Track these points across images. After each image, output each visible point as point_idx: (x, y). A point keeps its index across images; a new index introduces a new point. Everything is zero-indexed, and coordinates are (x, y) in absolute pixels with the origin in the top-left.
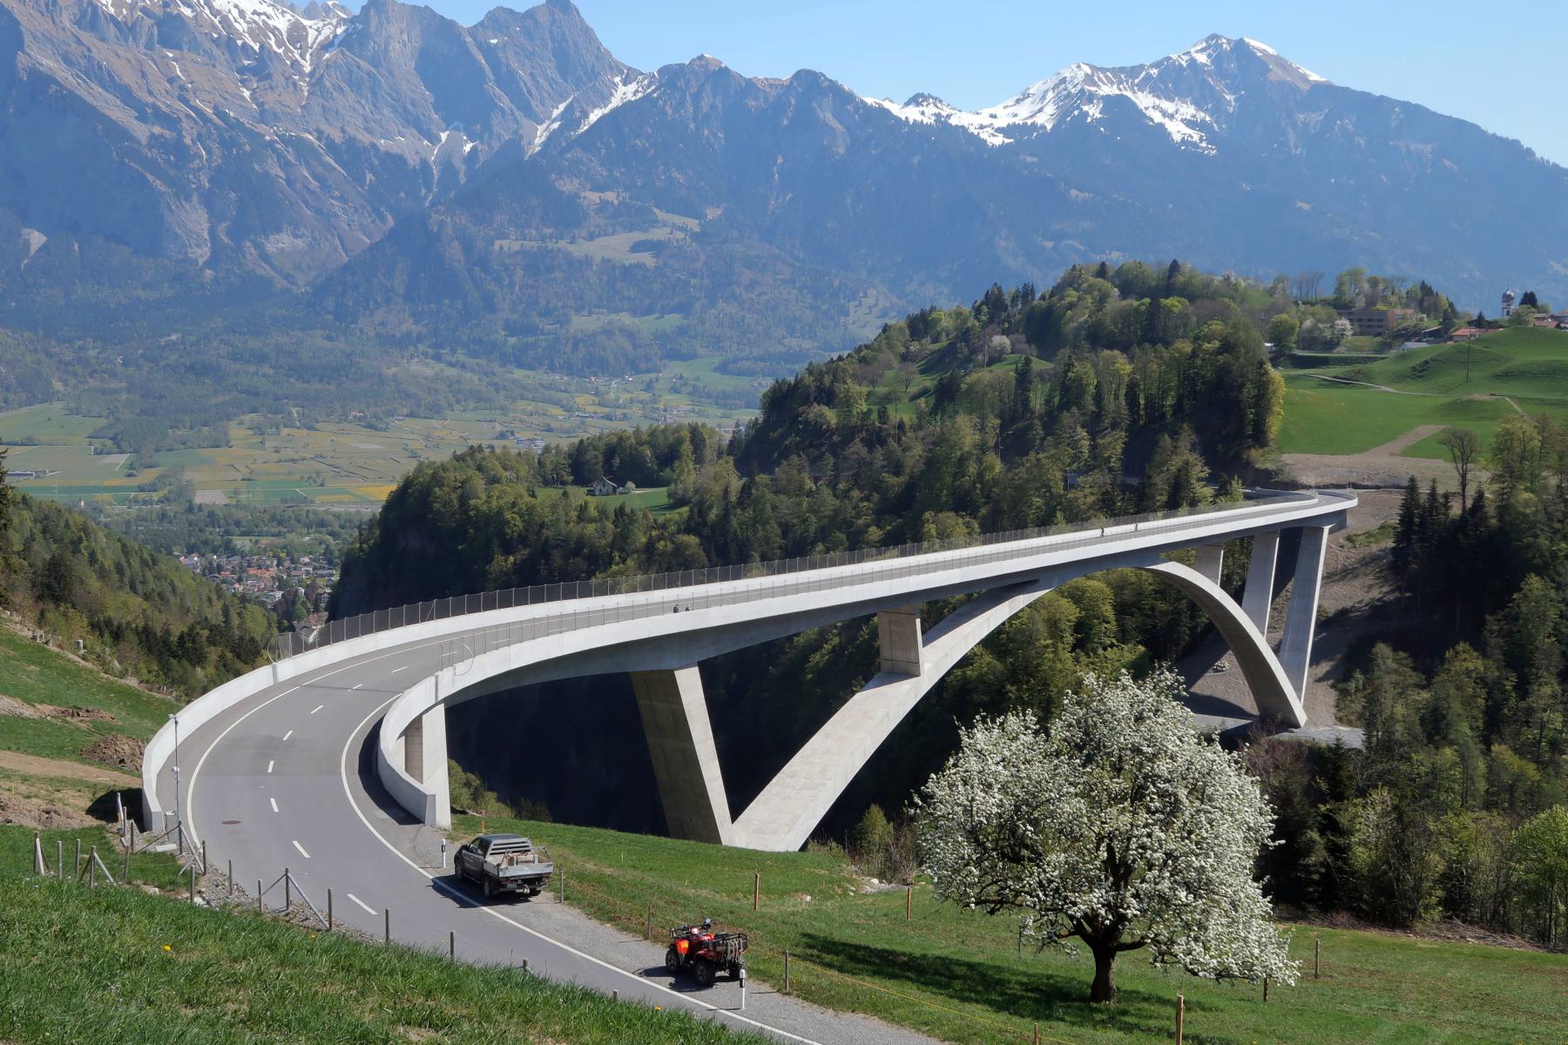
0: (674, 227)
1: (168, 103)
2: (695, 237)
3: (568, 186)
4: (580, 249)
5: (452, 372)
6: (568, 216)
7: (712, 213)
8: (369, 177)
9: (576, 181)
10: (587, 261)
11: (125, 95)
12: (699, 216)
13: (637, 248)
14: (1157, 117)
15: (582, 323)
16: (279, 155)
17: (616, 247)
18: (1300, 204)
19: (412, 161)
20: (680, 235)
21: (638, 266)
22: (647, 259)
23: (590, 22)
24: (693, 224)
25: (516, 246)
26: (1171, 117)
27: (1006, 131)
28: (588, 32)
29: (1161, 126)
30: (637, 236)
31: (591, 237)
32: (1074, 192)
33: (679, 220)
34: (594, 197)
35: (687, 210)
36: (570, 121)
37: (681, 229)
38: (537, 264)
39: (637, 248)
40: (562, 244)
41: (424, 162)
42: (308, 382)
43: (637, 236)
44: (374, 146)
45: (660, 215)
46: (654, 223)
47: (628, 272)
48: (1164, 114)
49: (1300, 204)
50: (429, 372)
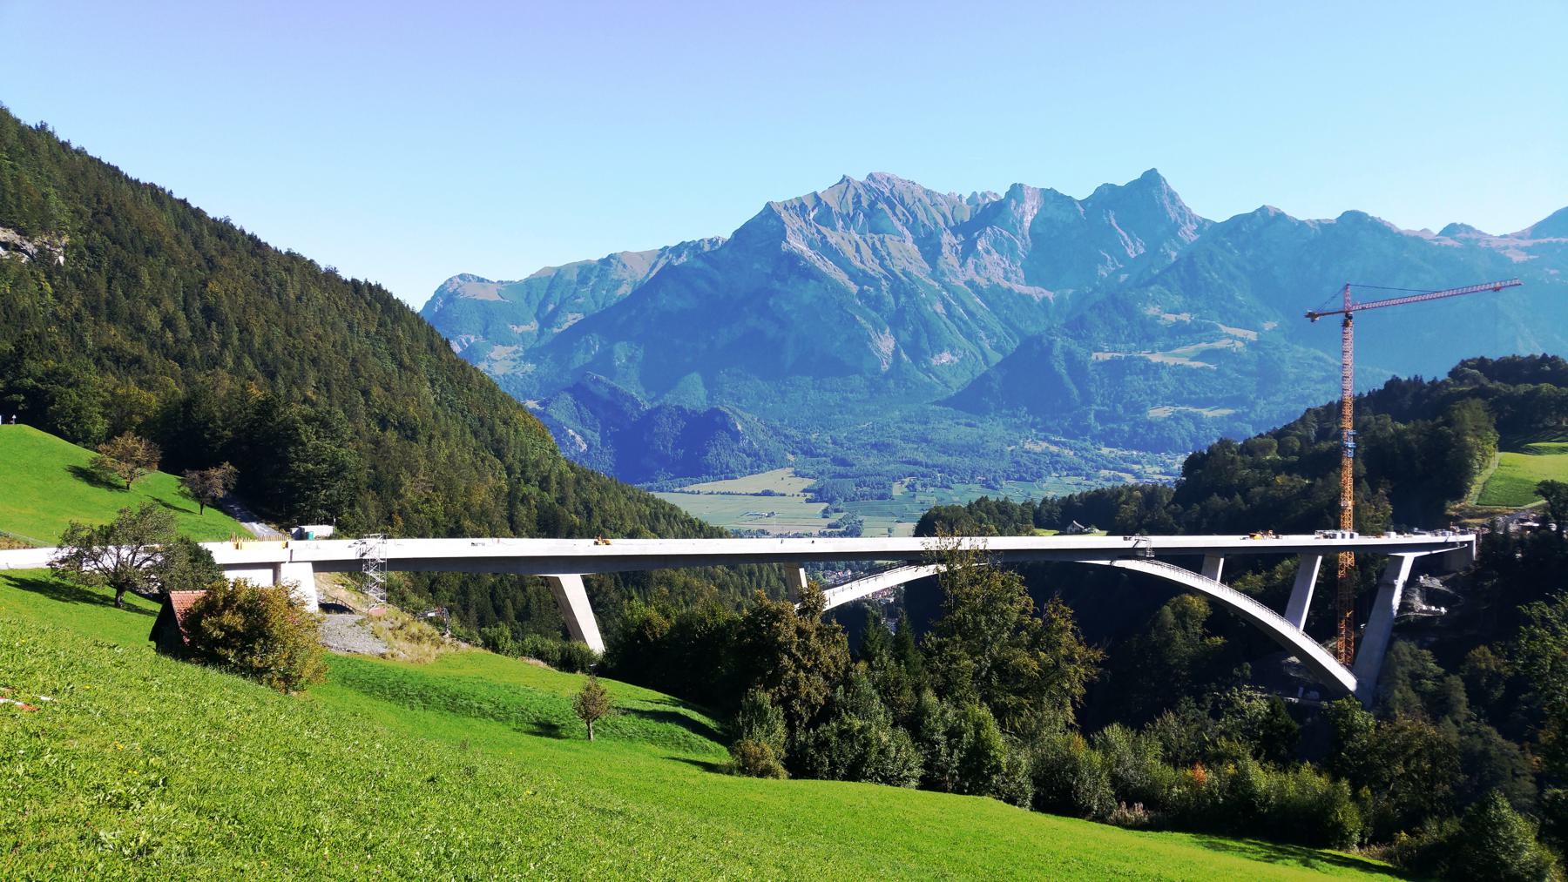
0: (1235, 338)
2: (1252, 346)
5: (1054, 449)
6: (1148, 334)
10: (1162, 365)
13: (1203, 356)
16: (943, 299)
23: (1175, 187)
24: (1252, 336)
25: (1108, 356)
28: (1173, 197)
33: (1240, 332)
34: (1172, 318)
37: (1242, 340)
38: (1116, 369)
42: (951, 455)
43: (1204, 346)
45: (1225, 329)
46: (1219, 337)
47: (1192, 373)
50: (1038, 449)
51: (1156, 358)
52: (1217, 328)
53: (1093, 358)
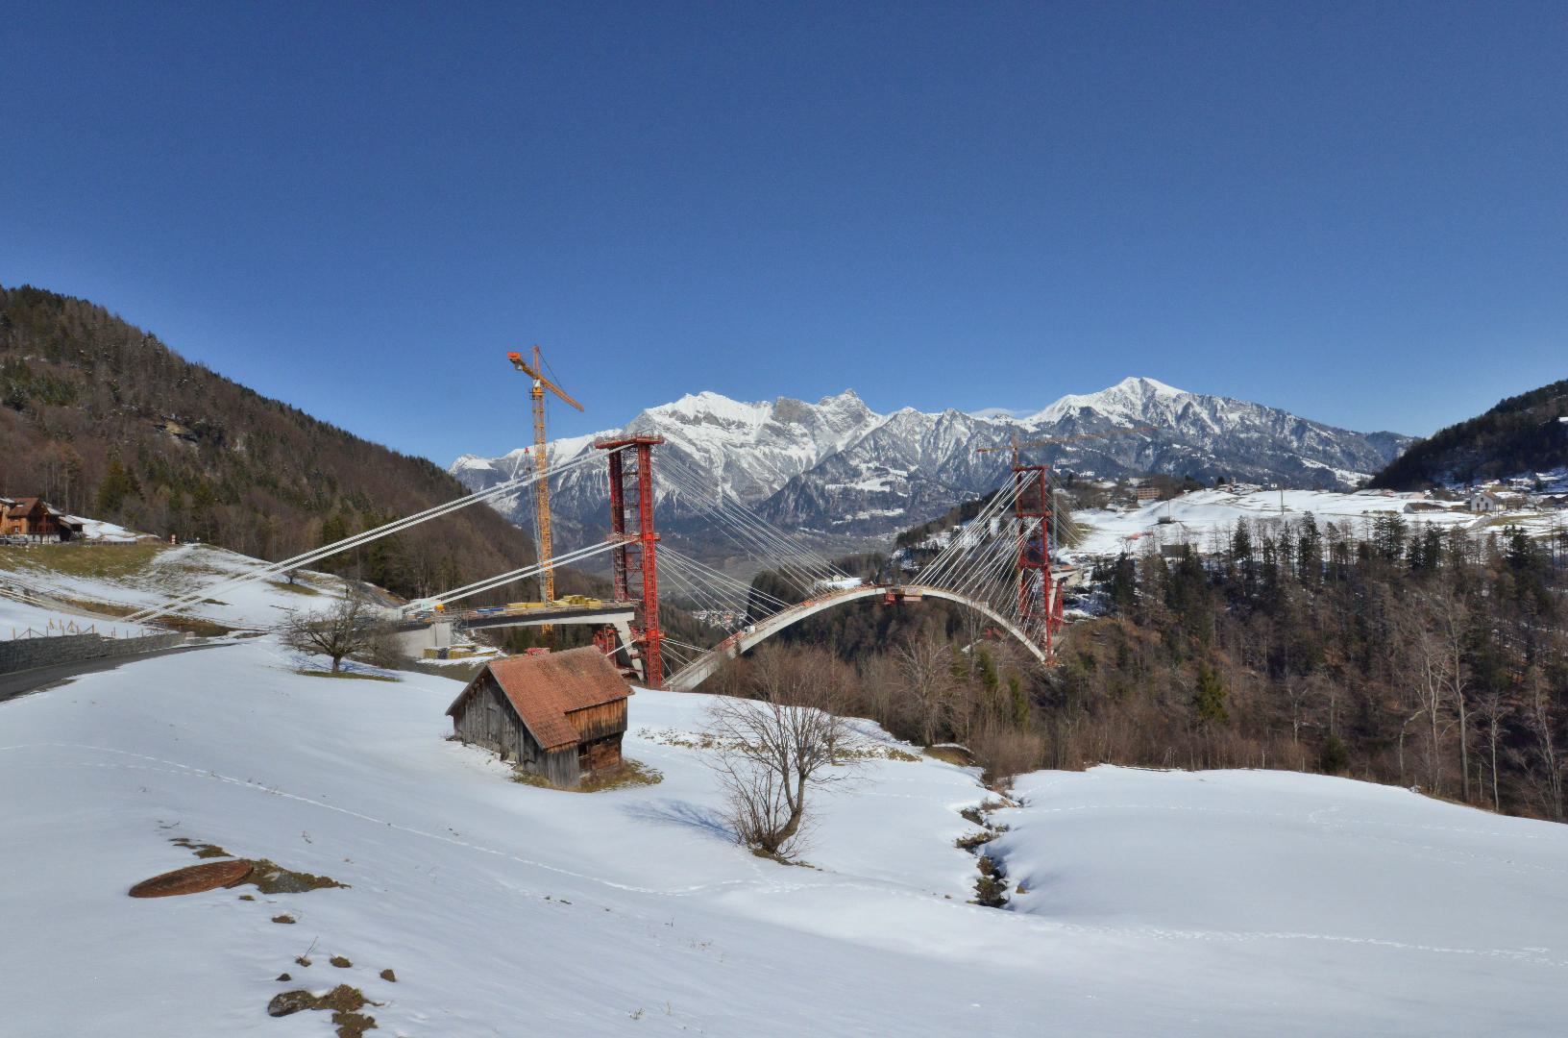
1: (705, 445)
3: (854, 463)
4: (861, 486)
6: (855, 474)
7: (913, 468)
8: (779, 464)
9: (857, 460)
10: (862, 491)
11: (690, 442)
12: (907, 470)
13: (882, 484)
14: (1105, 414)
15: (863, 515)
17: (873, 485)
18: (1175, 446)
19: (795, 457)
20: (899, 478)
21: (884, 492)
22: (887, 489)
24: (905, 474)
26: (1112, 414)
27: (1038, 425)
29: (1107, 418)
30: (883, 480)
31: (864, 481)
32: (1068, 449)
33: (899, 472)
35: (903, 468)
36: (856, 437)
39: (882, 484)
40: (853, 485)
41: (800, 459)
43: (883, 480)
44: (780, 453)
45: (892, 471)
47: (877, 493)
48: (1108, 412)
49: (1175, 446)
51: (858, 487)
52: (887, 470)
53: (827, 487)
